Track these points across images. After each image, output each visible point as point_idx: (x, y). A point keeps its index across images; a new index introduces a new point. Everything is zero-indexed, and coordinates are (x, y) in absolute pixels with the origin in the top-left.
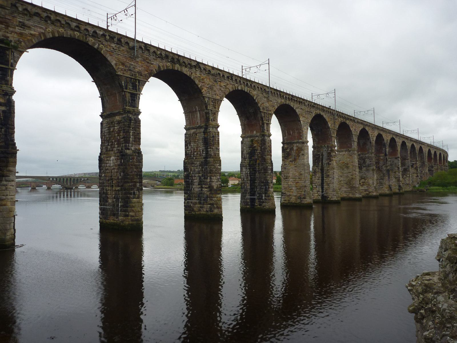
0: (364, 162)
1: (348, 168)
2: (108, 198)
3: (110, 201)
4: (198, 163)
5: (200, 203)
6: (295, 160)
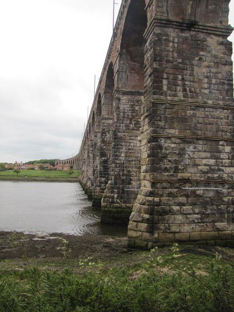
2: (131, 180)
3: (134, 183)
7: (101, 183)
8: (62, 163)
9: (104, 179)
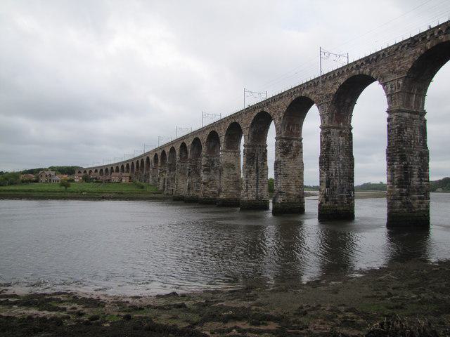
0: (213, 165)
1: (234, 169)
4: (417, 152)
5: (420, 198)
6: (294, 157)
7: (402, 195)
8: (96, 171)
9: (405, 190)
